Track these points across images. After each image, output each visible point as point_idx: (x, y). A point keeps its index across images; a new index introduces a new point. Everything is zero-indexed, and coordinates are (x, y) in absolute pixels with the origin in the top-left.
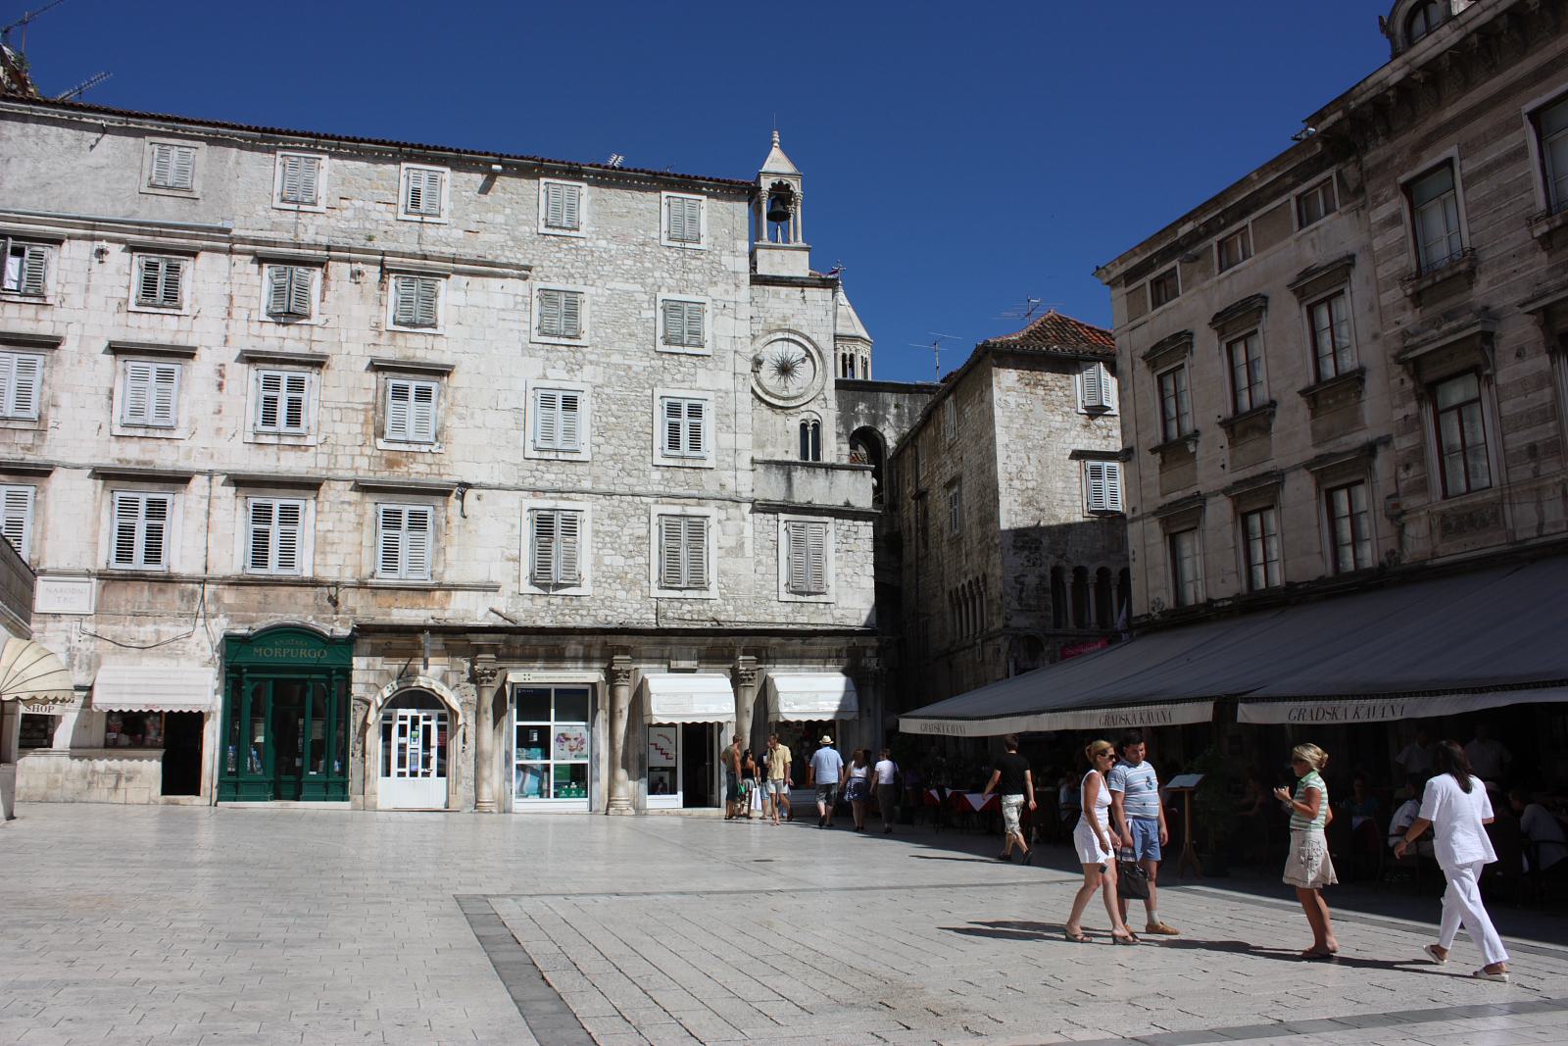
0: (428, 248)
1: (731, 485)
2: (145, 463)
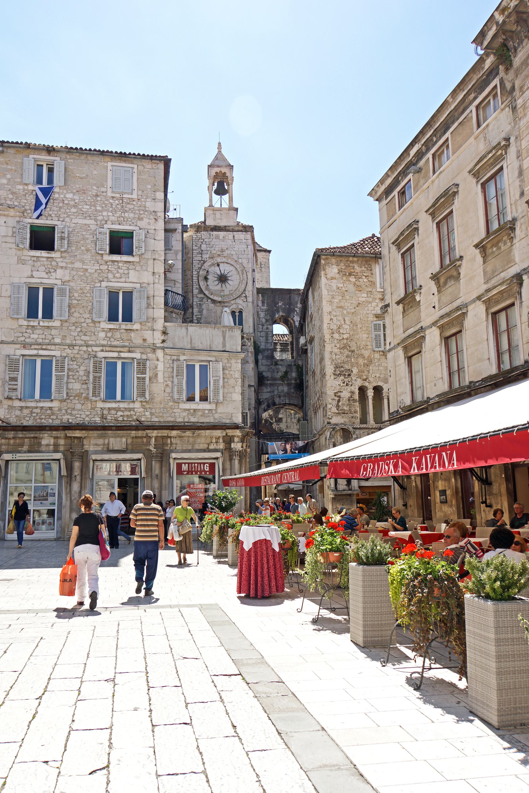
1: (150, 341)
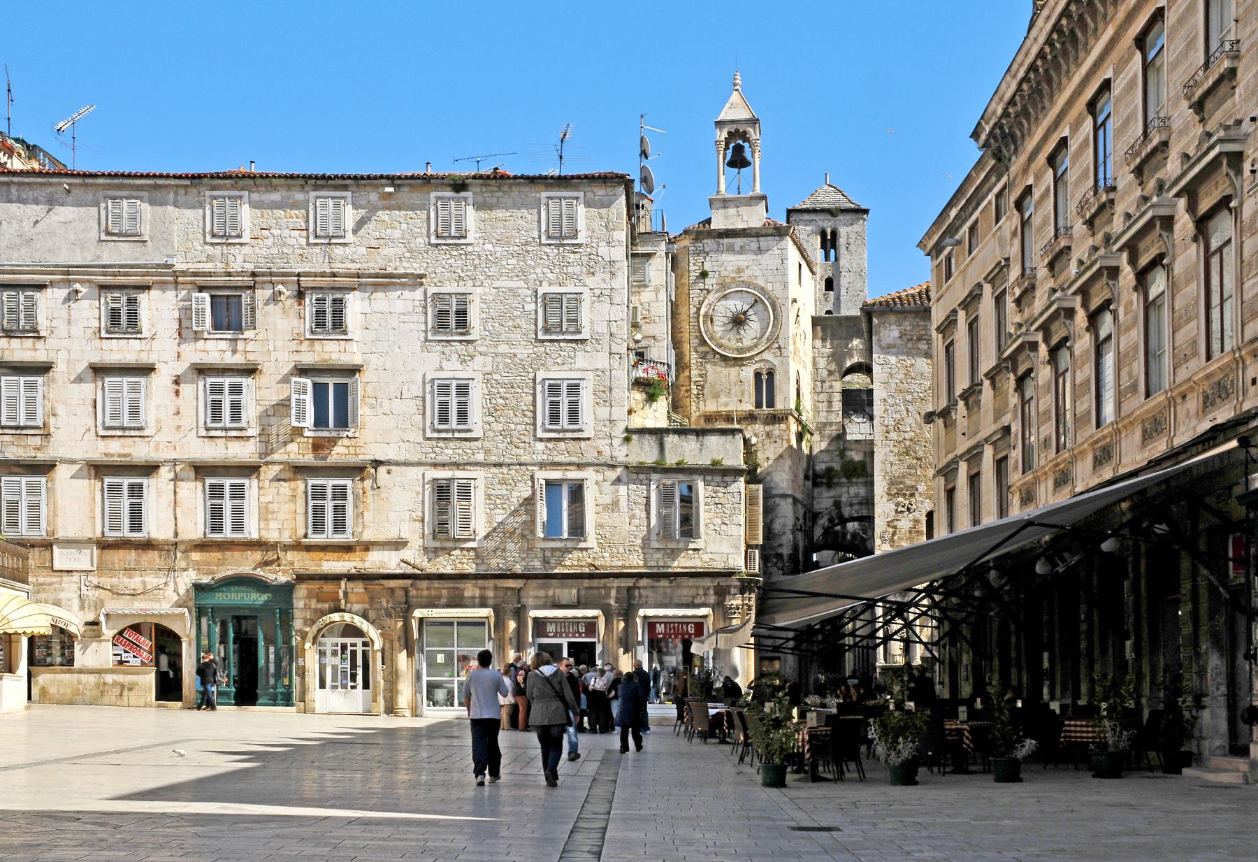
0: (338, 267)
2: (124, 456)
